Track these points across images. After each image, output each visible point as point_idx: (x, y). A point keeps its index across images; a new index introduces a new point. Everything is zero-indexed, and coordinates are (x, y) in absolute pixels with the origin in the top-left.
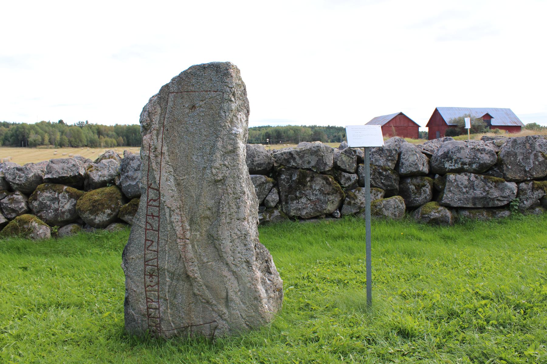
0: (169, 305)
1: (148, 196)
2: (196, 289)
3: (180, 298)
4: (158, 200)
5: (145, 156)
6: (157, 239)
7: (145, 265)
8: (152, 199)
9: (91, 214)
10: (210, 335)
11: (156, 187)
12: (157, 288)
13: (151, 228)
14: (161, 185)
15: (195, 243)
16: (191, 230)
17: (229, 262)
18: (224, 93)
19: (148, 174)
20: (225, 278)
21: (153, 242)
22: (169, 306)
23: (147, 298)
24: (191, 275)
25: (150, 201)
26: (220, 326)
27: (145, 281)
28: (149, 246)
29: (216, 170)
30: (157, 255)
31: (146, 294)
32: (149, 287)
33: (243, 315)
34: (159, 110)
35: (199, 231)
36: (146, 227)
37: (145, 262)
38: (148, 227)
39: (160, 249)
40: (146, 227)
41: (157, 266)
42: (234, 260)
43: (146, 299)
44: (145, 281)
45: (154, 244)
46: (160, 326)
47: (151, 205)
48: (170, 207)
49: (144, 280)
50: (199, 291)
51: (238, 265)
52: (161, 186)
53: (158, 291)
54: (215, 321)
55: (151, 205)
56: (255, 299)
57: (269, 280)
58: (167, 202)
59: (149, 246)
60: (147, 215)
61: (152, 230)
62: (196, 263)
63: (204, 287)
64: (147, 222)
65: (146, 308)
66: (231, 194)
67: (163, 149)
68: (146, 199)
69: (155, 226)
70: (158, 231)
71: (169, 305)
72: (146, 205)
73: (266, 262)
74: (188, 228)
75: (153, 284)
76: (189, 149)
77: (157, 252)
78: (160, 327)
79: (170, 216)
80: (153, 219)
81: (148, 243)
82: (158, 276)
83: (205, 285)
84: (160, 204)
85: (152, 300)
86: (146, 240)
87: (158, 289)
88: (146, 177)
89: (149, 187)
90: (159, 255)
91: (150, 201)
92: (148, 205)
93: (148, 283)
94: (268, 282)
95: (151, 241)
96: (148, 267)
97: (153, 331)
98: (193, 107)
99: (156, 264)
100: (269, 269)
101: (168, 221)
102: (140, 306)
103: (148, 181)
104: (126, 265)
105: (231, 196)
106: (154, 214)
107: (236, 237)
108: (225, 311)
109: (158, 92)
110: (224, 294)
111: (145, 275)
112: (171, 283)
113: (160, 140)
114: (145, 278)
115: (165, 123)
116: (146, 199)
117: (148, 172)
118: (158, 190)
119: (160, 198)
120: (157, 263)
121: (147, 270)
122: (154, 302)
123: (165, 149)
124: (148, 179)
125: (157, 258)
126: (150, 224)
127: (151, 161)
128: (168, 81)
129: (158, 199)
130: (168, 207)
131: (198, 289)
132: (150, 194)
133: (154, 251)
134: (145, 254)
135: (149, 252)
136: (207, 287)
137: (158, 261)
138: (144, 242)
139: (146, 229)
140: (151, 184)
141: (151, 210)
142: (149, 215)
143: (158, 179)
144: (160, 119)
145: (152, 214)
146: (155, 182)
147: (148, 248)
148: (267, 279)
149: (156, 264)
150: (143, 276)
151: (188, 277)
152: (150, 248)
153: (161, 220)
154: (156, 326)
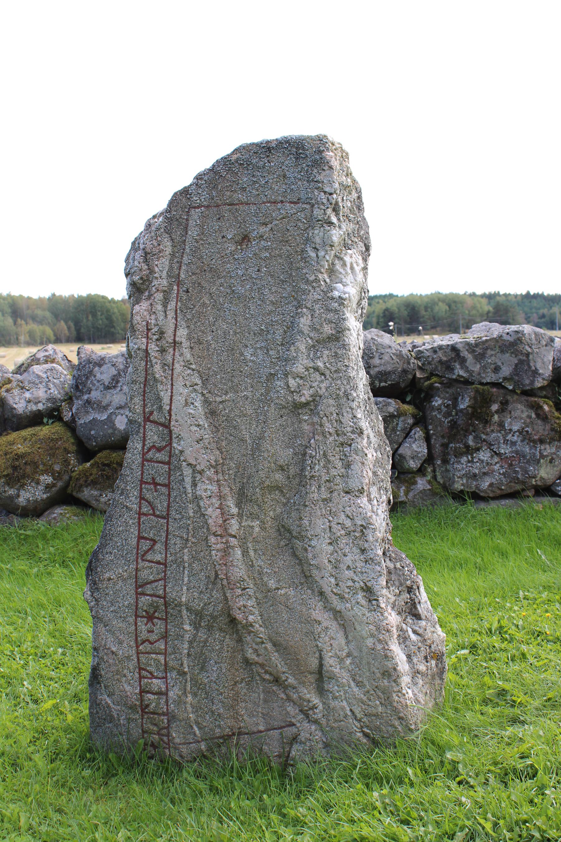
0: (189, 684)
1: (144, 440)
2: (250, 651)
3: (215, 669)
4: (168, 448)
5: (139, 349)
6: (164, 535)
7: (137, 593)
8: (154, 446)
9: (8, 485)
10: (279, 756)
11: (163, 420)
12: (163, 647)
13: (151, 512)
14: (173, 413)
15: (250, 545)
16: (240, 515)
17: (327, 589)
18: (313, 206)
19: (144, 391)
20: (316, 626)
21: (154, 542)
22: (188, 688)
23: (140, 669)
24: (239, 616)
25: (149, 450)
26: (303, 736)
27: (136, 629)
28: (146, 552)
29: (297, 379)
30: (165, 572)
31: (138, 660)
32: (146, 644)
33: (357, 711)
34: (167, 247)
35: (258, 518)
36: (140, 508)
37: (137, 589)
38: (145, 510)
39: (170, 558)
40: (140, 508)
41: (164, 598)
42: (337, 585)
43: (137, 670)
44: (136, 629)
45: (158, 546)
46: (169, 732)
47: (150, 461)
48: (194, 463)
49: (133, 628)
50: (258, 655)
51: (346, 596)
52: (173, 417)
53: (165, 654)
54: (293, 725)
55: (150, 461)
56: (383, 674)
57: (415, 632)
58: (188, 452)
59: (146, 552)
60: (142, 482)
61: (154, 514)
62: (251, 592)
63: (269, 646)
64: (142, 498)
65: (137, 691)
66: (330, 434)
67: (178, 334)
68: (141, 445)
69: (161, 507)
70: (167, 517)
71: (189, 684)
72: (140, 460)
73: (409, 592)
74: (235, 510)
75: (153, 637)
76: (235, 333)
77: (165, 565)
78: (168, 735)
79: (194, 485)
80: (156, 491)
81: (145, 545)
82: (166, 620)
83: (271, 640)
84: (170, 456)
85: (151, 673)
86: (140, 538)
87: (166, 649)
88: (141, 398)
89: (147, 419)
90: (168, 573)
91: (149, 450)
92: (144, 460)
93: (144, 635)
94: (413, 637)
95: (151, 540)
96: (143, 599)
97: (153, 745)
98: (243, 239)
99: (161, 592)
100: (416, 608)
101: (190, 495)
102: (125, 686)
103: (145, 406)
104: (95, 594)
105: (331, 439)
106: (158, 480)
107: (343, 532)
108: (316, 700)
109: (165, 206)
110: (314, 663)
111: (137, 616)
112: (195, 636)
113: (171, 314)
114: (136, 624)
115: (182, 276)
116: (139, 446)
117: (145, 385)
118: (167, 426)
119: (171, 444)
120: (165, 590)
121: (140, 605)
122: (156, 678)
123: (182, 333)
124: (144, 400)
125: (164, 579)
126: (149, 503)
127: (151, 361)
128: (187, 180)
129: (166, 446)
130: (189, 464)
131: (256, 651)
132: (149, 434)
133: (158, 563)
134: (137, 570)
135: (147, 564)
136: (275, 645)
137: (165, 586)
138: (134, 542)
139: (140, 514)
140: (151, 413)
141: (151, 470)
142: (146, 483)
143: (166, 400)
144: (171, 268)
145: (153, 479)
146: (160, 408)
147: (143, 556)
148: (410, 630)
149: (161, 592)
150: (131, 620)
151: (233, 621)
152: (149, 557)
153: (173, 494)
154: (158, 734)
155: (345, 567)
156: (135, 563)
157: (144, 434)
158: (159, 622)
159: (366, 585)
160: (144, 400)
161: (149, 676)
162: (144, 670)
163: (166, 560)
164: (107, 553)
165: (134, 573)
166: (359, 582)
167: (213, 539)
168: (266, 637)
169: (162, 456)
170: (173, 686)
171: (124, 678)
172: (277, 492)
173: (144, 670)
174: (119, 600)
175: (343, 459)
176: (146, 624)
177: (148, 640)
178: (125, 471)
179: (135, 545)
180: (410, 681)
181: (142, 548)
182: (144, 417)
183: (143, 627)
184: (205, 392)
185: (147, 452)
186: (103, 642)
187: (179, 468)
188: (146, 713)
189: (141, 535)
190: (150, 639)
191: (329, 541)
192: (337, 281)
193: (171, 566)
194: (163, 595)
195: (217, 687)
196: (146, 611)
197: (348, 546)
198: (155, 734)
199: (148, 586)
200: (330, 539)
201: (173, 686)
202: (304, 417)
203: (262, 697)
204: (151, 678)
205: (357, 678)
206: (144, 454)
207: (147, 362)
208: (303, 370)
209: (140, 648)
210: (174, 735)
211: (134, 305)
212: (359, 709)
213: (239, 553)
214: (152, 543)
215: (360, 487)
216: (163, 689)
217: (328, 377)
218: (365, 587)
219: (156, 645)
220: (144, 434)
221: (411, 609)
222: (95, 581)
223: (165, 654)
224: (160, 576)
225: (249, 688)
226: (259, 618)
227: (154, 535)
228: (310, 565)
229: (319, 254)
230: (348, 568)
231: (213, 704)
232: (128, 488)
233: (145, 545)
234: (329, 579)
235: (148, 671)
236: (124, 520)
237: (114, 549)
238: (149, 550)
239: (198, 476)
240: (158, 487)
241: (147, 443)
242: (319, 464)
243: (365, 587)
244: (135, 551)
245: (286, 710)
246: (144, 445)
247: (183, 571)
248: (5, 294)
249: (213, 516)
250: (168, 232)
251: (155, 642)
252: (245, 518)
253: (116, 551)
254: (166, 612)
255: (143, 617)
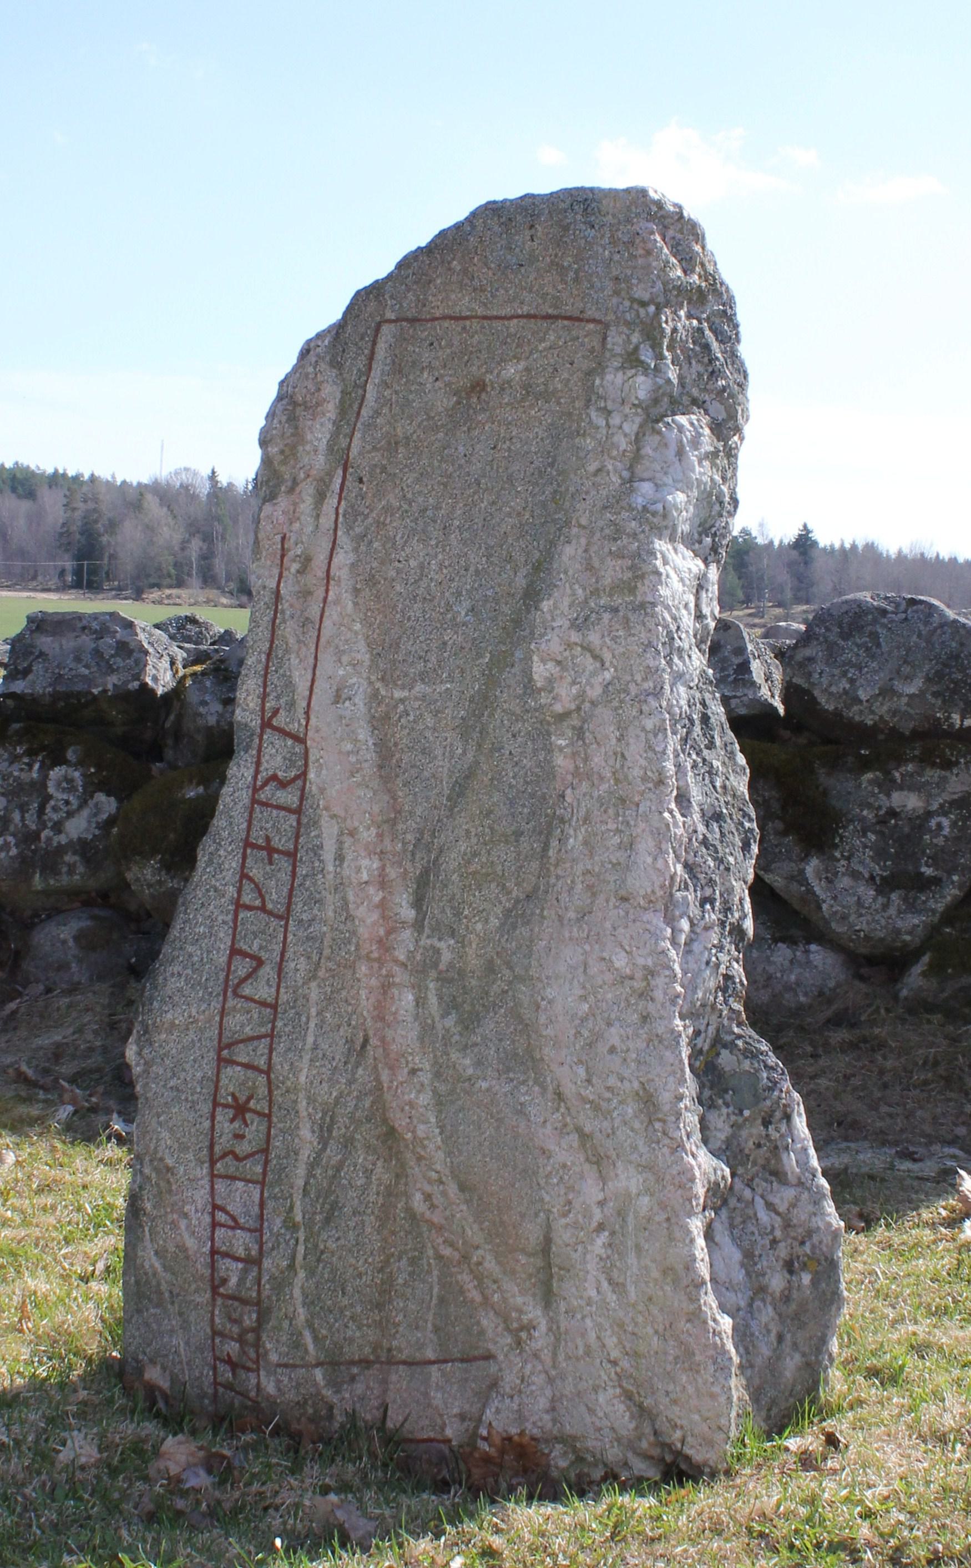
0: (301, 1249)
1: (258, 764)
2: (418, 1196)
3: (352, 1224)
4: (299, 783)
5: (264, 587)
6: (278, 948)
7: (220, 1059)
8: (274, 777)
9: (168, 870)
10: (462, 1417)
11: (294, 728)
12: (259, 1169)
13: (258, 903)
14: (312, 717)
15: (431, 985)
16: (418, 925)
17: (569, 1090)
18: (607, 326)
19: (267, 667)
20: (541, 1161)
21: (260, 962)
22: (300, 1257)
23: (215, 1207)
24: (400, 1122)
25: (265, 784)
26: (510, 1380)
27: (213, 1128)
28: (243, 980)
29: (550, 665)
30: (273, 1022)
31: (212, 1188)
32: (229, 1159)
33: (611, 1341)
34: (331, 392)
35: (453, 934)
36: (239, 892)
37: (220, 1049)
38: (247, 899)
39: (284, 997)
40: (239, 892)
41: (268, 1073)
42: (589, 1081)
43: (209, 1208)
44: (213, 1128)
45: (267, 971)
46: (258, 1338)
47: (265, 804)
48: (342, 814)
49: (207, 1124)
50: (433, 1207)
51: (604, 1105)
52: (313, 721)
53: (263, 1183)
54: (489, 1357)
55: (265, 804)
56: (665, 1272)
57: (770, 1206)
58: (332, 792)
59: (243, 980)
60: (248, 844)
61: (263, 908)
62: (425, 1077)
63: (452, 1189)
64: (244, 876)
65: (207, 1249)
66: (602, 778)
67: (335, 560)
68: (252, 771)
69: (275, 898)
70: (285, 917)
71: (301, 1249)
72: (246, 801)
73: (766, 1123)
74: (409, 914)
75: (244, 1148)
76: (441, 566)
77: (274, 1007)
78: (257, 1344)
79: (340, 858)
80: (271, 863)
81: (242, 967)
82: (269, 1116)
83: (454, 1175)
84: (302, 798)
85: (233, 1218)
86: (234, 952)
87: (264, 1173)
88: (260, 682)
89: (266, 724)
90: (279, 1024)
91: (265, 784)
92: (254, 801)
93: (224, 1142)
94: (764, 1216)
95: (252, 957)
96: (229, 1071)
97: (229, 1361)
98: (473, 388)
99: (262, 1062)
100: (779, 1160)
101: (331, 876)
102: (186, 1236)
103: (264, 697)
104: (146, 1051)
105: (605, 787)
106: (276, 843)
107: (608, 977)
108: (534, 1312)
109: (340, 316)
110: (532, 1233)
111: (215, 1104)
112: (319, 1154)
113: (327, 521)
114: (213, 1117)
115: (354, 451)
116: (249, 774)
117: (268, 660)
118: (300, 740)
119: (304, 774)
120: (270, 1059)
121: (224, 1081)
122: (242, 1229)
123: (343, 559)
124: (265, 686)
125: (271, 1036)
126: (257, 885)
127: (283, 612)
128: (382, 267)
129: (297, 778)
130: (334, 816)
131: (428, 1197)
132: (268, 750)
133: (263, 1004)
134: (222, 1013)
135: (240, 1003)
136: (462, 1188)
137: (271, 1051)
138: (223, 960)
139: (239, 905)
140: (276, 712)
141: (266, 822)
142: (255, 846)
143: (302, 686)
144: (335, 436)
145: (268, 839)
146: (292, 705)
147: (238, 985)
148: (759, 1202)
149: (262, 1062)
150: (206, 1108)
151: (391, 1133)
152: (247, 990)
153: (302, 870)
154: (241, 1340)
155: (605, 1050)
156: (221, 998)
157: (259, 751)
158: (257, 1119)
159: (645, 1089)
160: (265, 686)
161: (231, 1223)
162: (223, 1209)
163: (277, 999)
164: (173, 975)
165: (217, 1018)
166: (630, 1082)
167: (363, 968)
168: (447, 1172)
169: (288, 797)
170: (273, 1249)
171: (185, 1221)
172: (493, 885)
173: (223, 1209)
174: (187, 1066)
175: (621, 831)
176: (232, 1121)
177: (232, 1152)
178: (219, 822)
179: (224, 965)
180: (742, 1304)
181: (235, 971)
182: (262, 719)
183: (226, 1125)
184: (373, 678)
185: (262, 787)
186: (152, 1146)
187: (315, 823)
188: (222, 1295)
189: (237, 946)
190: (237, 1150)
191: (581, 992)
192: (645, 475)
193: (285, 1011)
194: (265, 1068)
195: (353, 1261)
196: (233, 1095)
197: (616, 1007)
198: (233, 1339)
199: (241, 1046)
200: (584, 987)
201: (273, 1249)
202: (560, 742)
203: (436, 1290)
204: (232, 1228)
205: (615, 1274)
206: (255, 790)
207: (276, 612)
208: (562, 649)
209: (218, 1165)
210: (268, 1346)
211: (263, 504)
212: (615, 1339)
213: (411, 997)
214: (254, 964)
215: (649, 890)
216: (253, 1253)
217: (607, 664)
218: (641, 1093)
219: (248, 1164)
220: (259, 751)
221: (768, 1160)
222: (147, 1026)
223: (263, 1183)
224: (263, 1030)
225: (414, 1272)
226: (437, 1131)
227: (261, 948)
228: (541, 1036)
229: (611, 422)
230: (612, 1050)
231: (344, 1293)
232: (222, 852)
233: (242, 967)
234: (575, 1068)
235: (227, 1213)
236: (208, 913)
237: (185, 968)
238: (249, 976)
239: (348, 841)
240: (276, 856)
241: (262, 769)
242: (576, 837)
243: (641, 1093)
244: (222, 975)
245: (478, 1323)
246: (257, 772)
247: (307, 1023)
248: (9, 464)
249: (369, 921)
250: (336, 364)
251: (247, 1157)
252: (427, 930)
253: (189, 971)
254: (270, 1101)
255: (226, 1106)
